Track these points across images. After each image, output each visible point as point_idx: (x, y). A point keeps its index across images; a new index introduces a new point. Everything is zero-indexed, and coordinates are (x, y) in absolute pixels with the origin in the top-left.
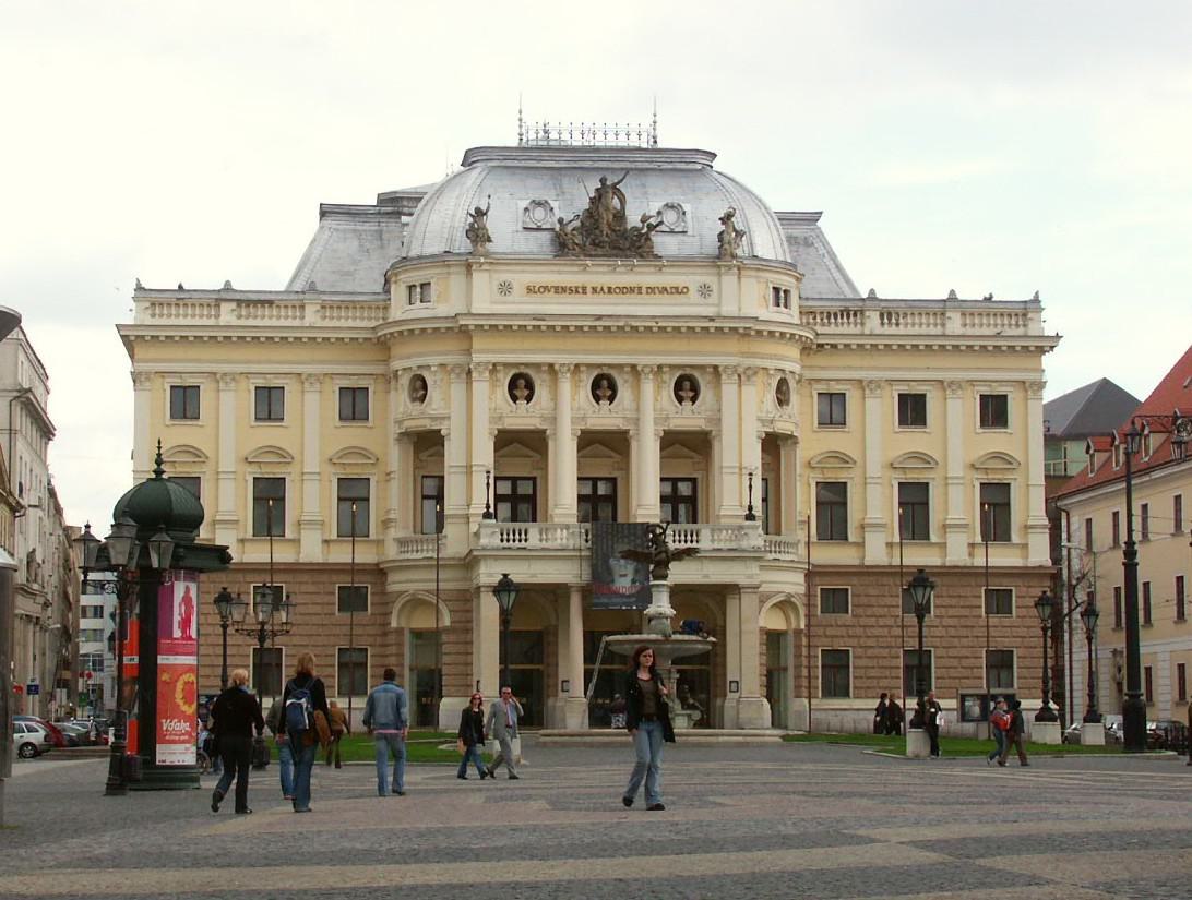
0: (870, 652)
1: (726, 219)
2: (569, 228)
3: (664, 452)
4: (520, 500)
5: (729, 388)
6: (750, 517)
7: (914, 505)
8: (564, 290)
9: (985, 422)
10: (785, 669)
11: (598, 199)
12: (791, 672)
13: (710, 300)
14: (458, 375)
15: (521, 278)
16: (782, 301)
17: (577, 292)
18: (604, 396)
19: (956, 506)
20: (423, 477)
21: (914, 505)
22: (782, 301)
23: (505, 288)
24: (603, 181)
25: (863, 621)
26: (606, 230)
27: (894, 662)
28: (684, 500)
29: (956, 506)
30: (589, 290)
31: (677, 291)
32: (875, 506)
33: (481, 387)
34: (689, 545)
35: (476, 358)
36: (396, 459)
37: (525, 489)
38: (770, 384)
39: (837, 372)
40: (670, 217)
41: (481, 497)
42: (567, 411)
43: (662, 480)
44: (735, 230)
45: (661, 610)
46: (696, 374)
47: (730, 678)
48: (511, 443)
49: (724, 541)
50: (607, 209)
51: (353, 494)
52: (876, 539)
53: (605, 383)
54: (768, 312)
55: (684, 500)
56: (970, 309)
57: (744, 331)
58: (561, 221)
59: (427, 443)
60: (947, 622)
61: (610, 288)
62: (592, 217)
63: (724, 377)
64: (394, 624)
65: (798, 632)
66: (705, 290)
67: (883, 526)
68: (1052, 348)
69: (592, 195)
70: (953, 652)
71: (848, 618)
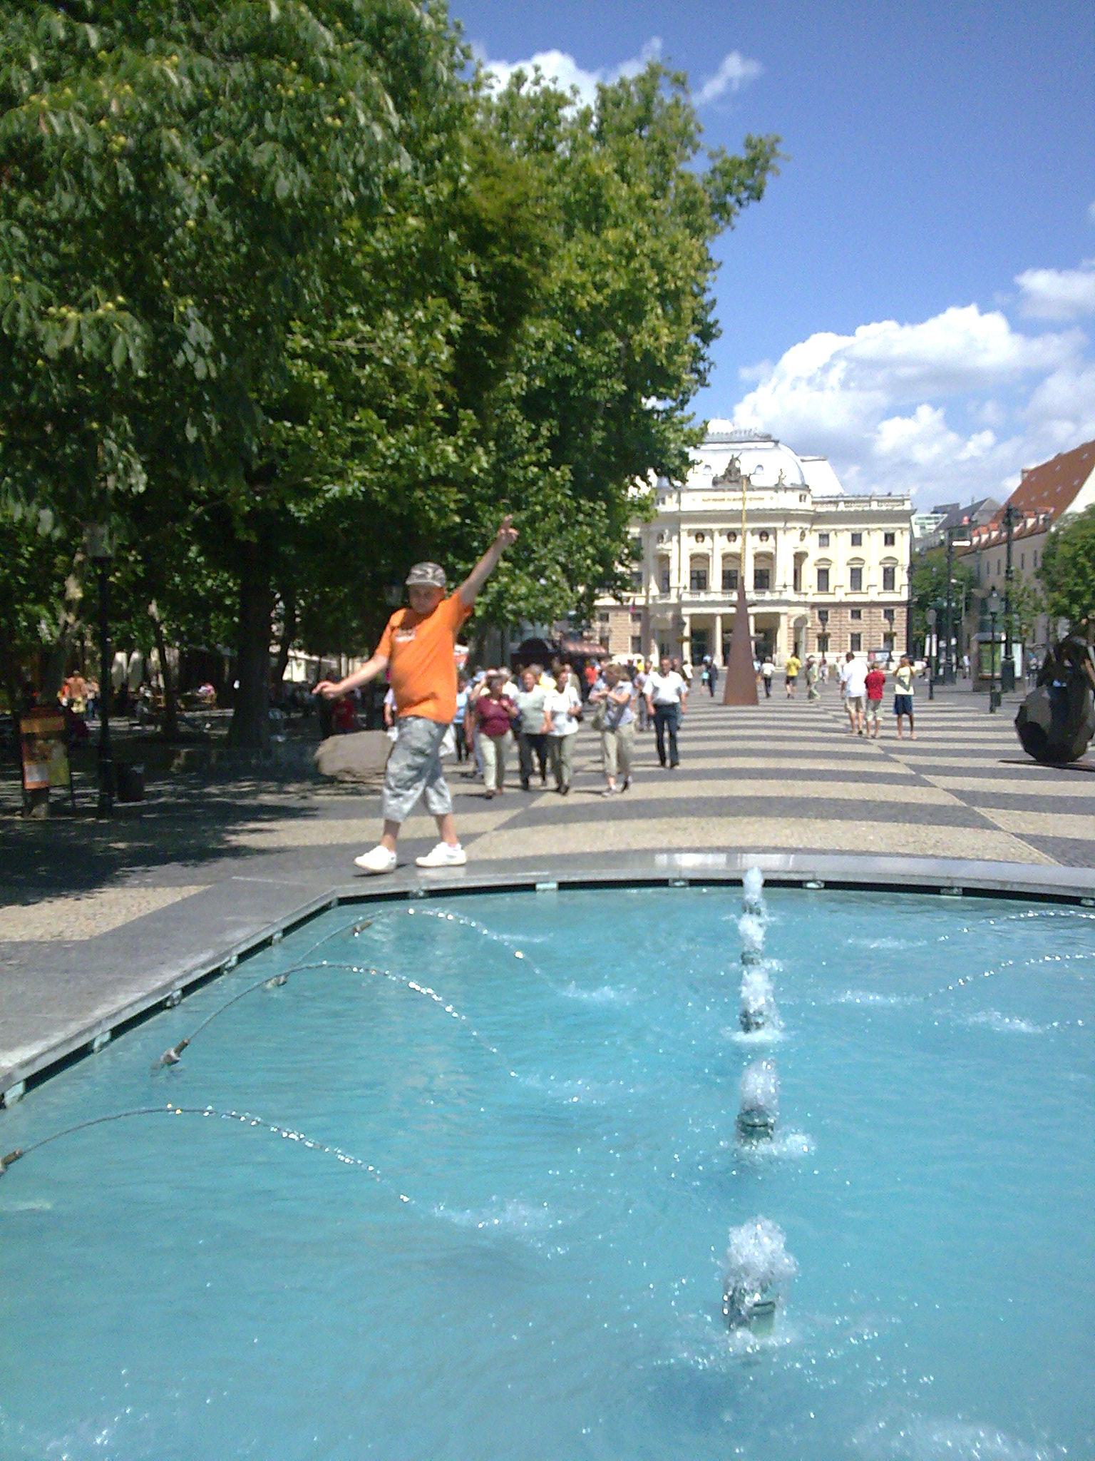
4: (699, 581)
5: (780, 533)
7: (856, 576)
9: (886, 543)
11: (732, 462)
19: (873, 576)
21: (856, 576)
29: (873, 576)
32: (840, 576)
37: (702, 575)
41: (686, 580)
42: (718, 546)
49: (776, 597)
52: (840, 589)
55: (763, 580)
59: (665, 559)
62: (729, 471)
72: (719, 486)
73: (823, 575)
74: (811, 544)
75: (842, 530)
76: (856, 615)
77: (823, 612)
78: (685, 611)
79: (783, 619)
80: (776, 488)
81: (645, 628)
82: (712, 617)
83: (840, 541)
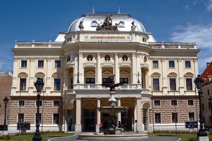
0: (165, 114)
1: (133, 23)
2: (100, 25)
3: (121, 73)
4: (90, 81)
5: (134, 58)
6: (139, 82)
7: (173, 83)
8: (99, 37)
10: (147, 117)
12: (149, 118)
13: (130, 39)
14: (77, 55)
15: (90, 36)
16: (145, 41)
17: (102, 38)
18: (107, 60)
20: (71, 78)
21: (173, 83)
22: (145, 41)
23: (86, 37)
24: (107, 17)
25: (163, 107)
26: (108, 26)
27: (170, 116)
28: (124, 81)
30: (104, 38)
31: (122, 37)
32: (165, 83)
33: (81, 58)
34: (125, 89)
35: (80, 51)
36: (66, 74)
37: (92, 80)
38: (143, 57)
39: (155, 57)
40: (121, 25)
43: (120, 78)
44: (135, 26)
45: (113, 100)
46: (127, 55)
47: (135, 119)
48: (89, 71)
50: (108, 22)
51: (58, 83)
53: (107, 57)
54: (141, 42)
55: (124, 81)
56: (182, 45)
57: (137, 47)
58: (98, 24)
59: (71, 70)
60: (180, 107)
61: (108, 37)
62: (105, 24)
63: (133, 55)
64: (64, 108)
65: (150, 110)
66: (128, 37)
67: (167, 87)
68: (199, 52)
69: (105, 19)
70: (182, 113)
71: (160, 107)
72: (100, 31)
73: (156, 82)
74: (149, 63)
75: (164, 59)
76: (174, 103)
77: (157, 100)
78: (78, 96)
79: (138, 101)
80: (130, 33)
81: (60, 109)
82: (95, 100)
83: (164, 66)
